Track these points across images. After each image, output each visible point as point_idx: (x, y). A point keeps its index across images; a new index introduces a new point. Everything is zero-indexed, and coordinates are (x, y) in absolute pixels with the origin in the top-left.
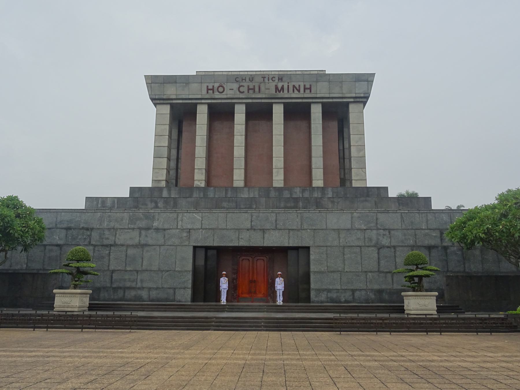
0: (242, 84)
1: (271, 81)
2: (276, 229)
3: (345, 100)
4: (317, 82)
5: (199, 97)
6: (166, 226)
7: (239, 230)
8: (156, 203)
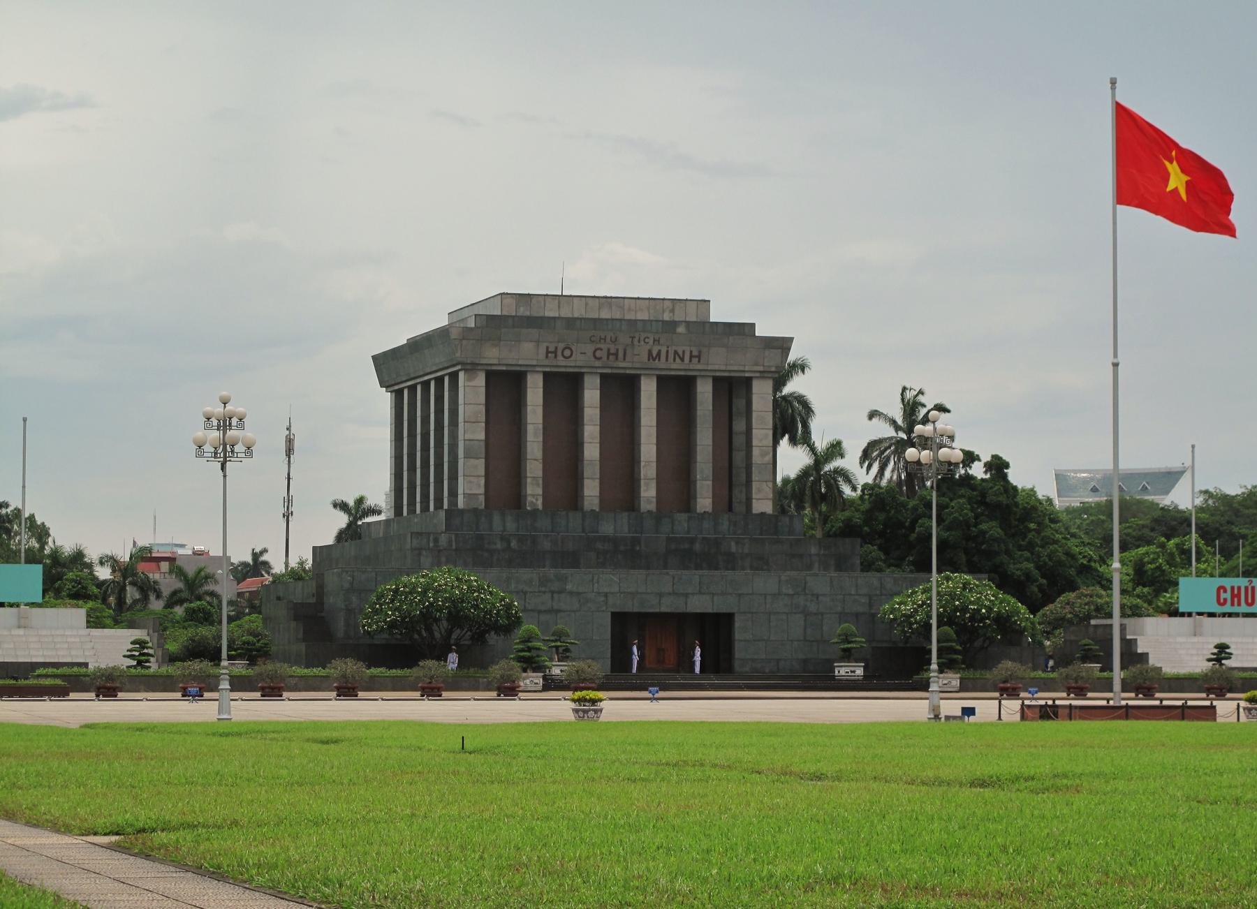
2: (700, 593)
3: (747, 375)
5: (534, 363)
6: (581, 590)
7: (661, 595)
8: (509, 542)
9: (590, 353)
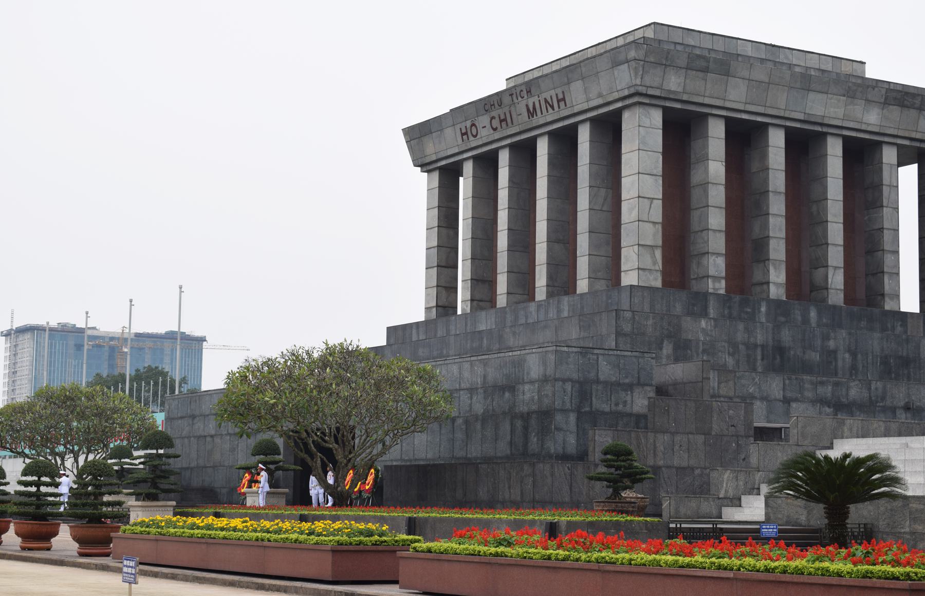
0: (494, 114)
1: (520, 99)
3: (612, 108)
4: (569, 83)
9: (488, 126)
